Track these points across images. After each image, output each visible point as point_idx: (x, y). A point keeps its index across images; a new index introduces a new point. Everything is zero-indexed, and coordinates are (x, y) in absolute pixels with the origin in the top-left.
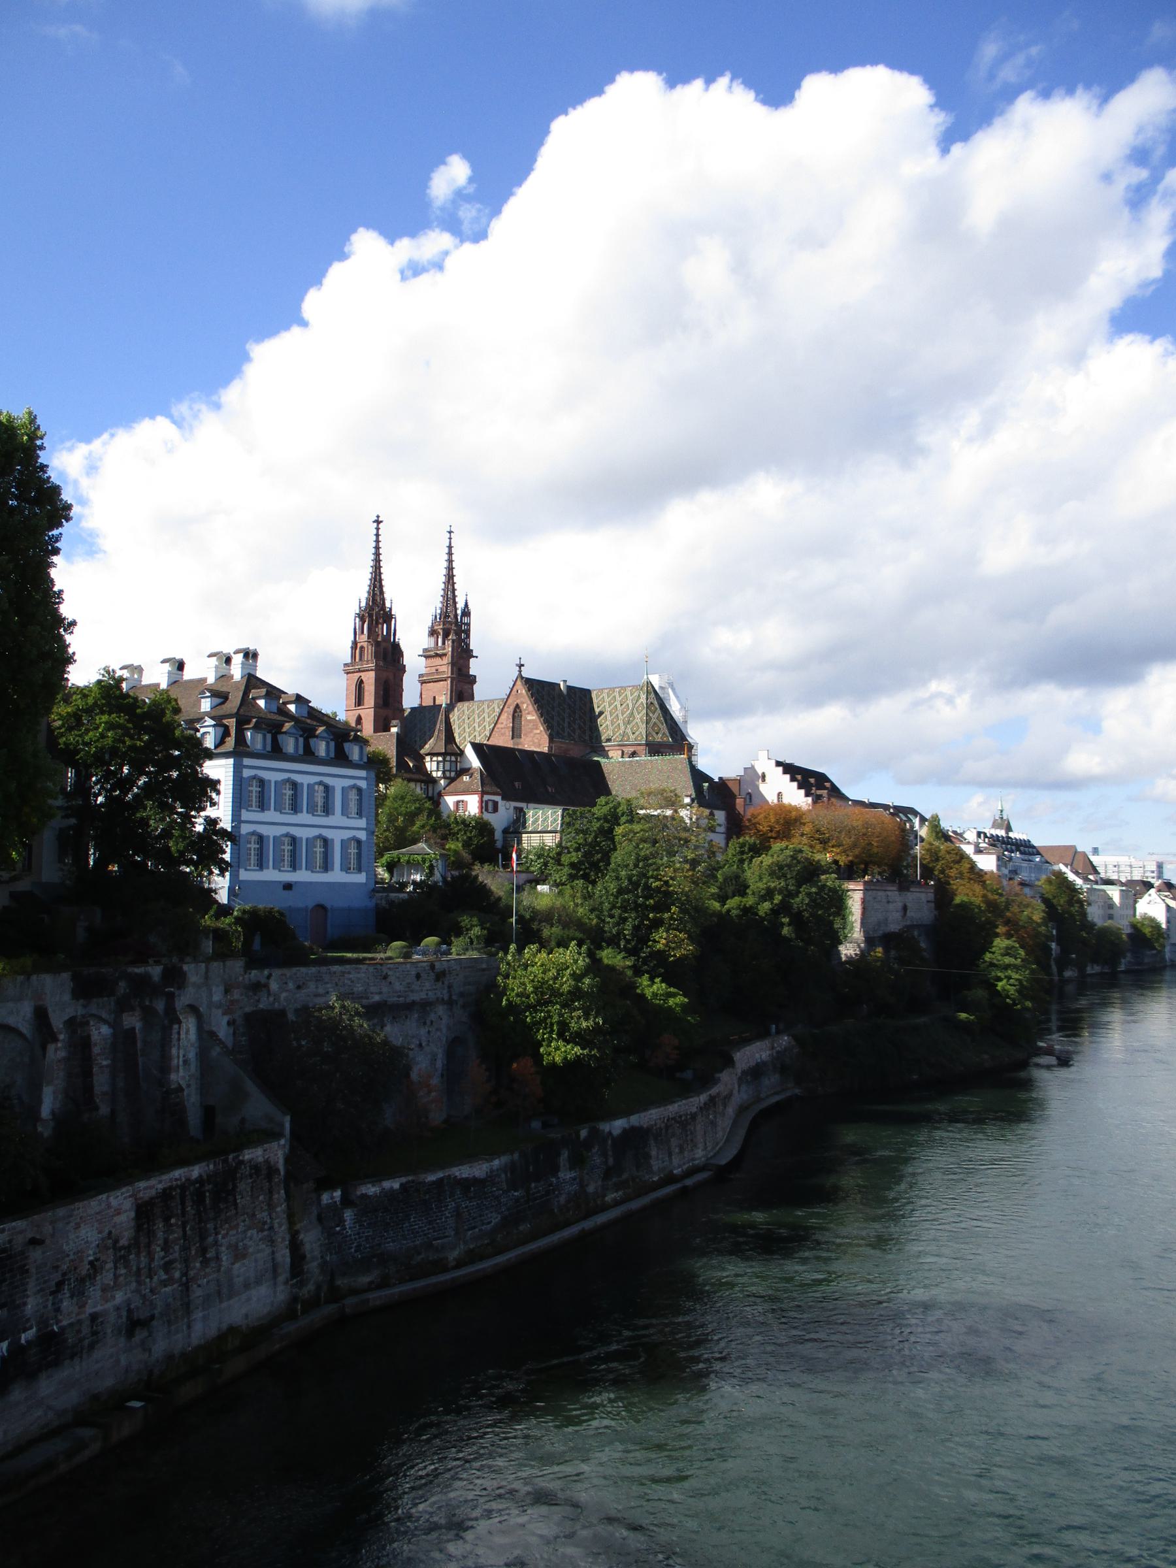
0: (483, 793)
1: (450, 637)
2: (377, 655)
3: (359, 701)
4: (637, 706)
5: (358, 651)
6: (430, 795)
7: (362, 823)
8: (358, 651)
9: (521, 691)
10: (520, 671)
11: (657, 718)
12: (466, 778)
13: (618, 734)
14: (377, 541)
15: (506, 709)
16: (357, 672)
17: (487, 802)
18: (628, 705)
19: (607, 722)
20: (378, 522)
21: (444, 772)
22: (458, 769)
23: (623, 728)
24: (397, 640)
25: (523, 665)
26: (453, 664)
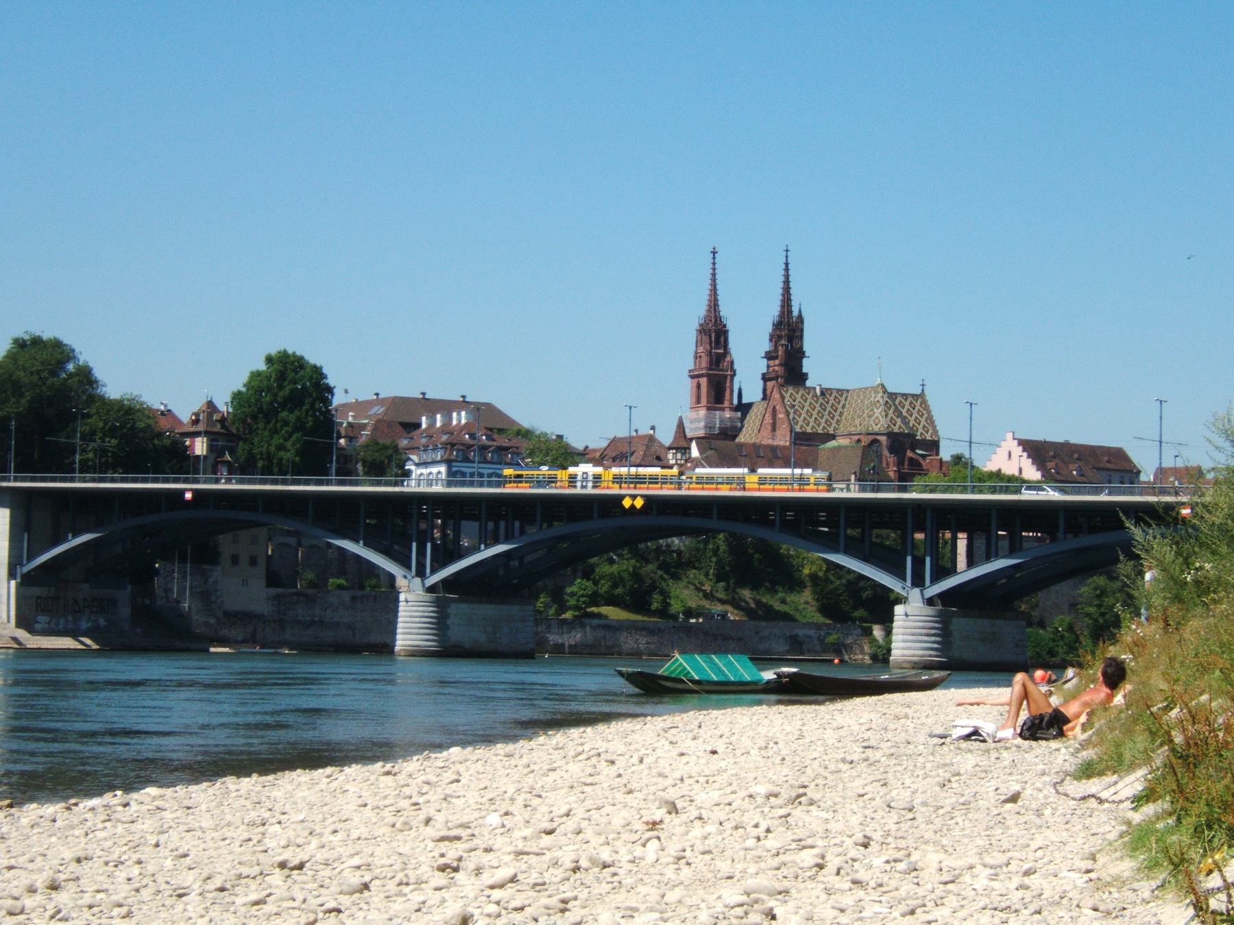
14: (714, 269)
20: (714, 253)
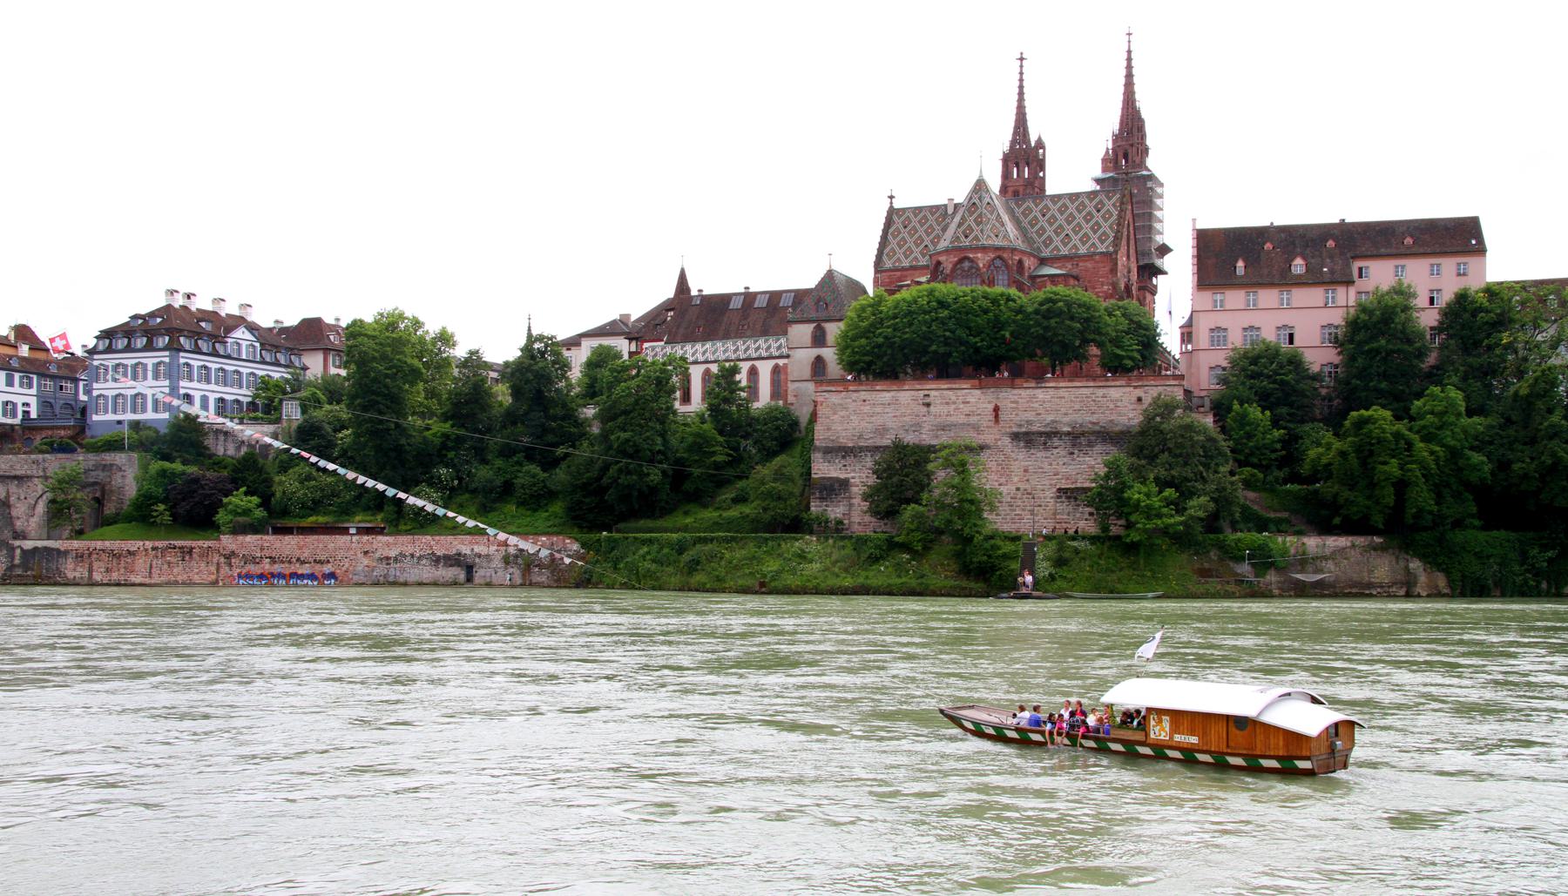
7: (167, 383)
10: (891, 203)
20: (1022, 59)
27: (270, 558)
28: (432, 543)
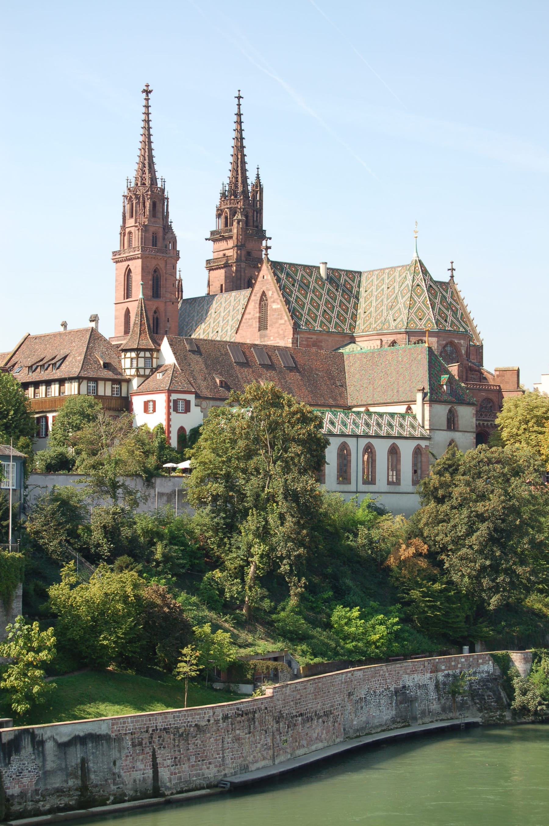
0: (170, 392)
1: (235, 218)
2: (144, 240)
3: (128, 293)
4: (402, 288)
5: (126, 238)
6: (124, 394)
8: (126, 238)
9: (267, 276)
11: (423, 302)
12: (159, 376)
13: (379, 322)
15: (253, 298)
16: (125, 261)
17: (176, 402)
18: (394, 288)
19: (372, 309)
20: (147, 92)
21: (138, 369)
22: (155, 366)
23: (385, 314)
24: (170, 224)
25: (270, 248)
26: (239, 247)
27: (301, 715)
28: (387, 674)
